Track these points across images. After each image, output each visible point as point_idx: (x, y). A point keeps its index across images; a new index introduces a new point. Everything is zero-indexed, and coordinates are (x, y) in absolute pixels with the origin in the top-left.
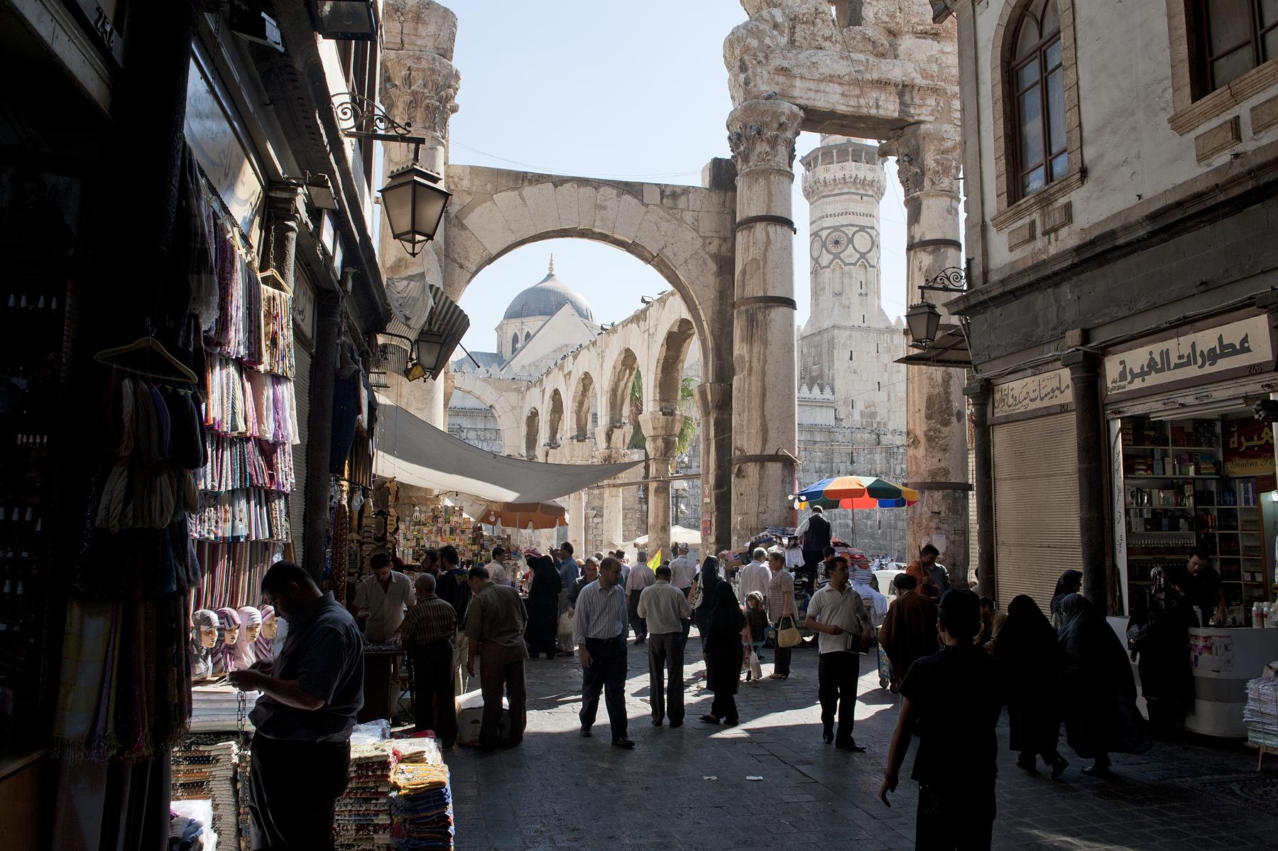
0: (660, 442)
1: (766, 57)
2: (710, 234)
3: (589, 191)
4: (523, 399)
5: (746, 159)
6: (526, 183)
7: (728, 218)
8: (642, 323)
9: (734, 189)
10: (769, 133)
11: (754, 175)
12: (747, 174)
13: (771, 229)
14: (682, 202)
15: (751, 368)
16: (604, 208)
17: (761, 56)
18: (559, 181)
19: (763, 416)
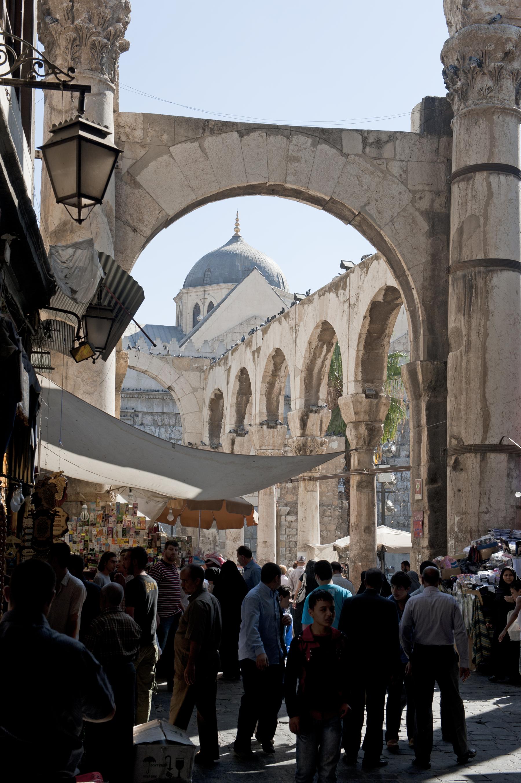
0: (363, 429)
2: (420, 187)
3: (279, 140)
4: (206, 379)
5: (464, 96)
6: (207, 133)
7: (443, 168)
8: (341, 292)
9: (449, 133)
10: (492, 65)
11: (473, 116)
12: (465, 115)
13: (494, 179)
14: (388, 151)
15: (469, 343)
16: (297, 160)
18: (245, 130)
19: (484, 399)
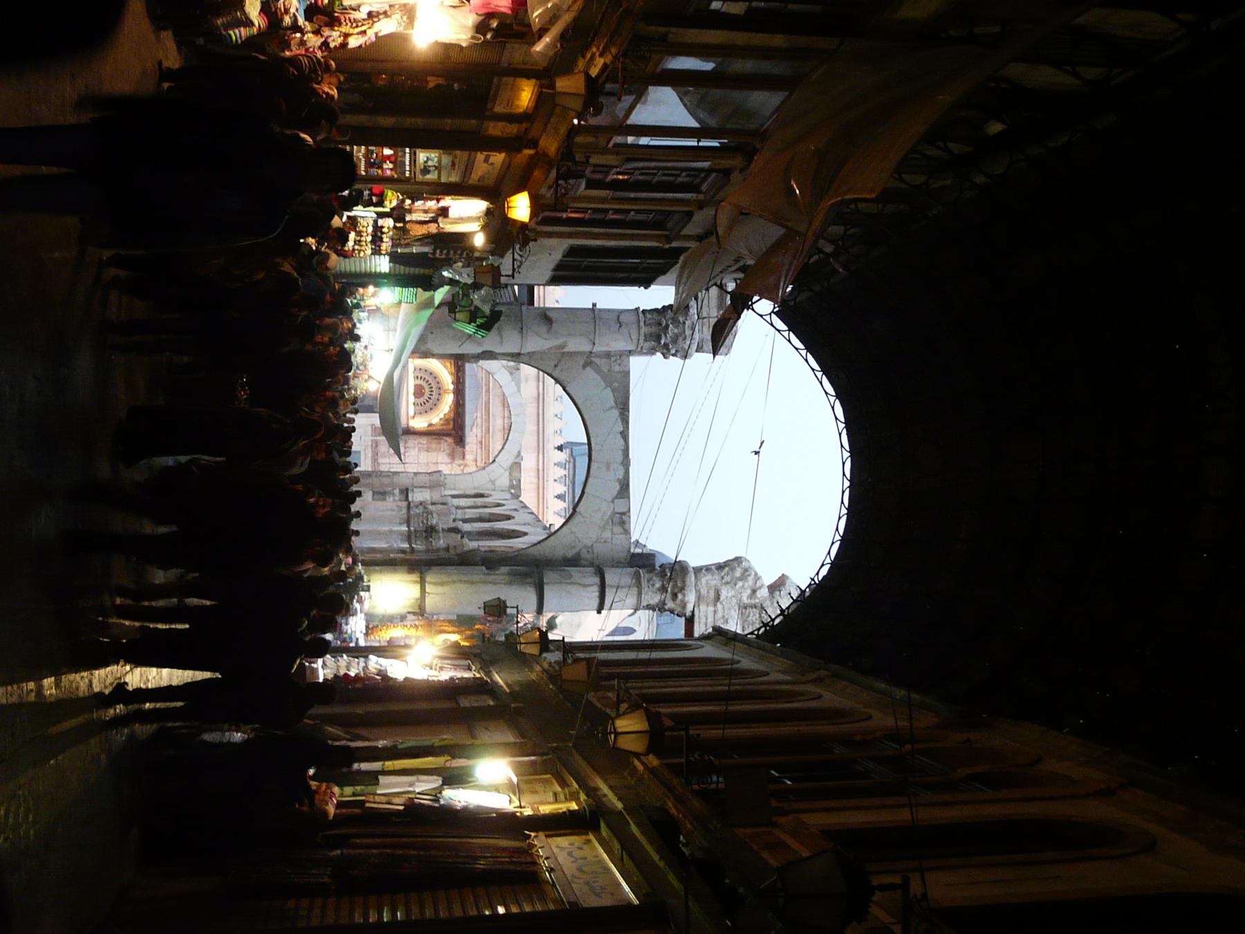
1: (727, 583)
3: (620, 458)
14: (618, 529)
17: (727, 579)
18: (625, 435)
